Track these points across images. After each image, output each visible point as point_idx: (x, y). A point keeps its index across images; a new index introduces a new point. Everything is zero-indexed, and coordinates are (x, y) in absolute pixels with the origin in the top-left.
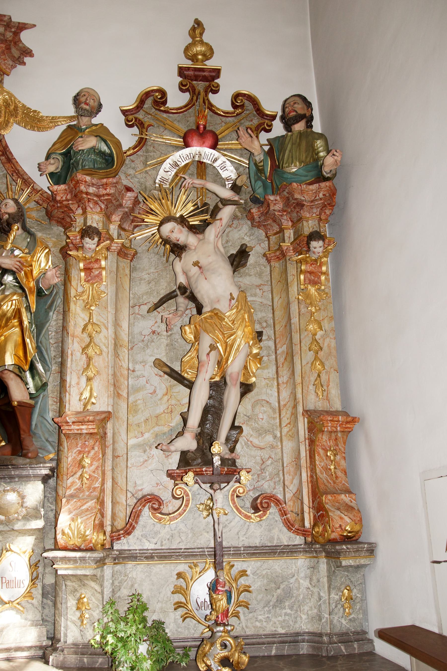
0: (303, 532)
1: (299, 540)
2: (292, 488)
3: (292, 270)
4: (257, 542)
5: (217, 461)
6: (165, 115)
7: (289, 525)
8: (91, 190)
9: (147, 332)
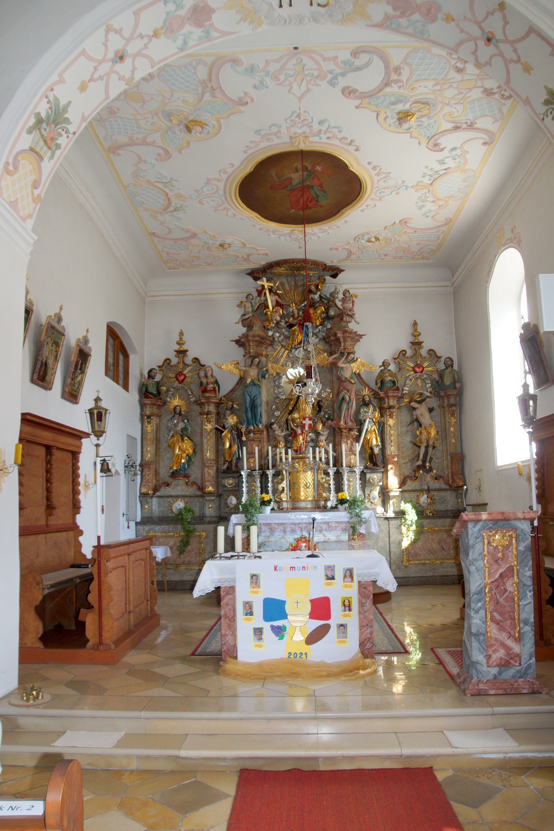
0: (450, 485)
1: (448, 487)
2: (446, 474)
3: (447, 413)
4: (437, 487)
5: (428, 467)
6: (406, 359)
7: (445, 483)
8: (391, 394)
9: (405, 430)
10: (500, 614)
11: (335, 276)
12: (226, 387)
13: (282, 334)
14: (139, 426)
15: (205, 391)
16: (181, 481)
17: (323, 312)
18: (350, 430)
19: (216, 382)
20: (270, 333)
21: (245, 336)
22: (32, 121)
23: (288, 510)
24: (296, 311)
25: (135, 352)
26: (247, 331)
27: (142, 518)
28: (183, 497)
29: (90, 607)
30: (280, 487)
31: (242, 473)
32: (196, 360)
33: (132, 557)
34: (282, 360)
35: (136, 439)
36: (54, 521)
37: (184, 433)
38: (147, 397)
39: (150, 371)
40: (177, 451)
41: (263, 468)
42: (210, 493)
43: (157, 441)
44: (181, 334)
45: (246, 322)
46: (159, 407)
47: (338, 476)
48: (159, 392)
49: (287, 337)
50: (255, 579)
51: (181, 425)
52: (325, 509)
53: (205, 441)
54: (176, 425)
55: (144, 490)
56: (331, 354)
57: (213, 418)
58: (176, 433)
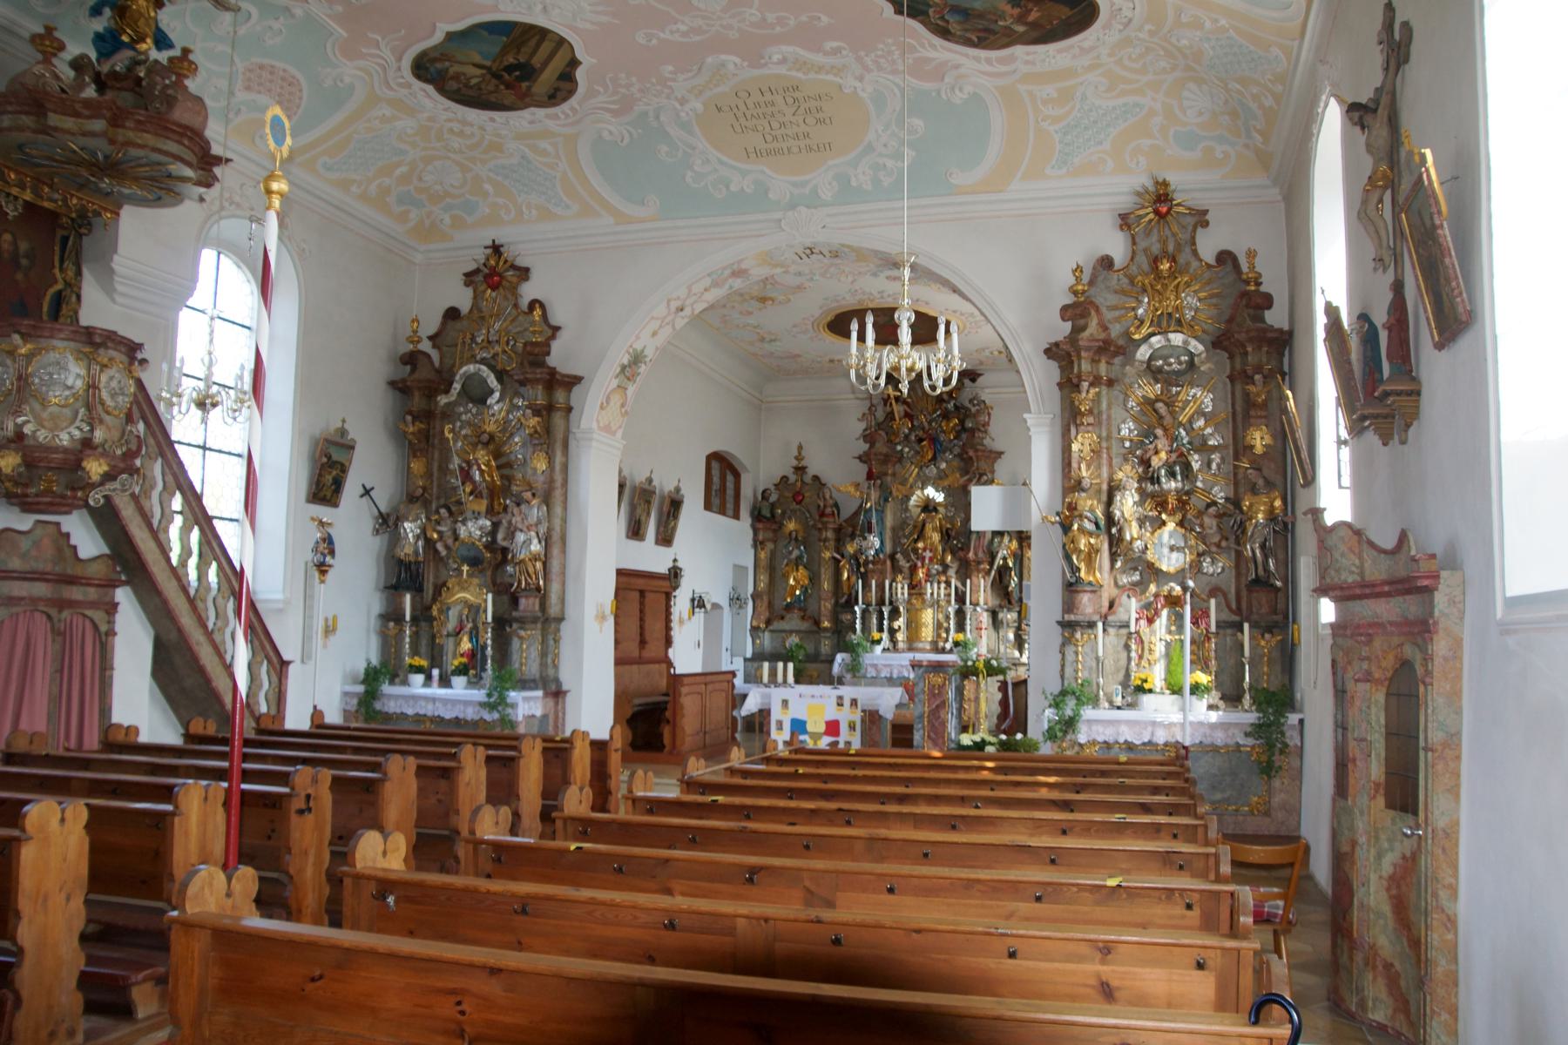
10: (936, 734)
11: (973, 380)
12: (847, 511)
13: (911, 448)
14: (752, 552)
15: (822, 515)
16: (796, 614)
17: (956, 425)
18: (979, 563)
19: (836, 505)
20: (899, 448)
21: (867, 454)
22: (619, 370)
23: (903, 651)
24: (926, 424)
25: (746, 470)
26: (871, 447)
27: (754, 654)
28: (798, 632)
29: (668, 722)
30: (896, 625)
31: (856, 608)
32: (816, 478)
33: (710, 687)
34: (911, 480)
35: (747, 568)
36: (647, 654)
37: (797, 562)
38: (759, 521)
39: (764, 492)
40: (792, 582)
41: (881, 602)
42: (826, 629)
43: (772, 569)
44: (800, 448)
45: (868, 437)
46: (775, 531)
47: (960, 614)
48: (773, 516)
49: (917, 453)
50: (785, 703)
51: (796, 553)
52: (943, 651)
53: (823, 570)
54: (791, 553)
55: (755, 624)
56: (962, 476)
57: (832, 544)
58: (790, 561)
